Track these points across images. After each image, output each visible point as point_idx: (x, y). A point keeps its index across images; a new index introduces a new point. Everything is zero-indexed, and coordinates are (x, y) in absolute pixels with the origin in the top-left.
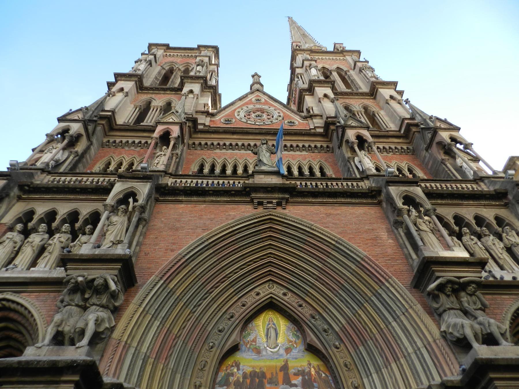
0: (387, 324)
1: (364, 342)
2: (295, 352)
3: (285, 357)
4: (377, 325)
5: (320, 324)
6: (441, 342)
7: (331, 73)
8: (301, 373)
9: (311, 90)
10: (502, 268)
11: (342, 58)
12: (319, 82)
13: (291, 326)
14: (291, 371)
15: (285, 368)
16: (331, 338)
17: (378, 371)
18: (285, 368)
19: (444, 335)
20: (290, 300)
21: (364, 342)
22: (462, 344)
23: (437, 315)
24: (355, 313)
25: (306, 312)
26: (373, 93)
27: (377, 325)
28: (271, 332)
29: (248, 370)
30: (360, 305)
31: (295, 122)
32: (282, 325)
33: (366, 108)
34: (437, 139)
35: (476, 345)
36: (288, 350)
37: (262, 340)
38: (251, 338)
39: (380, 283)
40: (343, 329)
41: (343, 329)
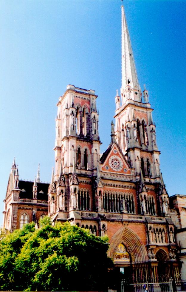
0: (141, 252)
1: (136, 253)
2: (124, 252)
3: (123, 252)
4: (139, 251)
5: (129, 248)
6: (147, 256)
7: (140, 126)
8: (125, 255)
9: (133, 149)
10: (159, 242)
11: (146, 111)
12: (137, 148)
13: (124, 247)
14: (124, 255)
15: (123, 255)
16: (131, 251)
17: (137, 257)
18: (123, 255)
19: (148, 255)
20: (125, 243)
21: (136, 253)
22: (149, 258)
23: (148, 252)
24: (136, 248)
25: (127, 245)
26: (152, 152)
27: (139, 251)
28: (121, 248)
29: (118, 255)
30: (137, 247)
31: (127, 170)
32: (123, 247)
33: (148, 159)
34: (161, 196)
35: (151, 258)
36: (124, 251)
37: (120, 250)
38: (118, 249)
39: (141, 245)
40: (133, 250)
41: (133, 250)
